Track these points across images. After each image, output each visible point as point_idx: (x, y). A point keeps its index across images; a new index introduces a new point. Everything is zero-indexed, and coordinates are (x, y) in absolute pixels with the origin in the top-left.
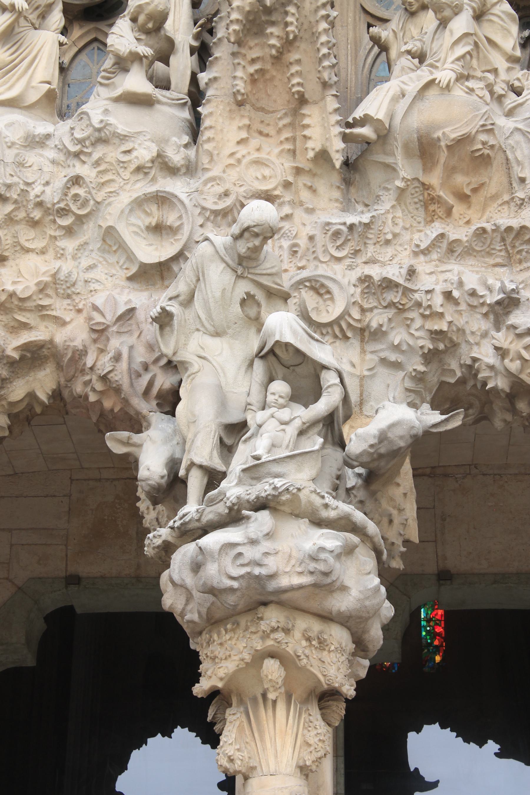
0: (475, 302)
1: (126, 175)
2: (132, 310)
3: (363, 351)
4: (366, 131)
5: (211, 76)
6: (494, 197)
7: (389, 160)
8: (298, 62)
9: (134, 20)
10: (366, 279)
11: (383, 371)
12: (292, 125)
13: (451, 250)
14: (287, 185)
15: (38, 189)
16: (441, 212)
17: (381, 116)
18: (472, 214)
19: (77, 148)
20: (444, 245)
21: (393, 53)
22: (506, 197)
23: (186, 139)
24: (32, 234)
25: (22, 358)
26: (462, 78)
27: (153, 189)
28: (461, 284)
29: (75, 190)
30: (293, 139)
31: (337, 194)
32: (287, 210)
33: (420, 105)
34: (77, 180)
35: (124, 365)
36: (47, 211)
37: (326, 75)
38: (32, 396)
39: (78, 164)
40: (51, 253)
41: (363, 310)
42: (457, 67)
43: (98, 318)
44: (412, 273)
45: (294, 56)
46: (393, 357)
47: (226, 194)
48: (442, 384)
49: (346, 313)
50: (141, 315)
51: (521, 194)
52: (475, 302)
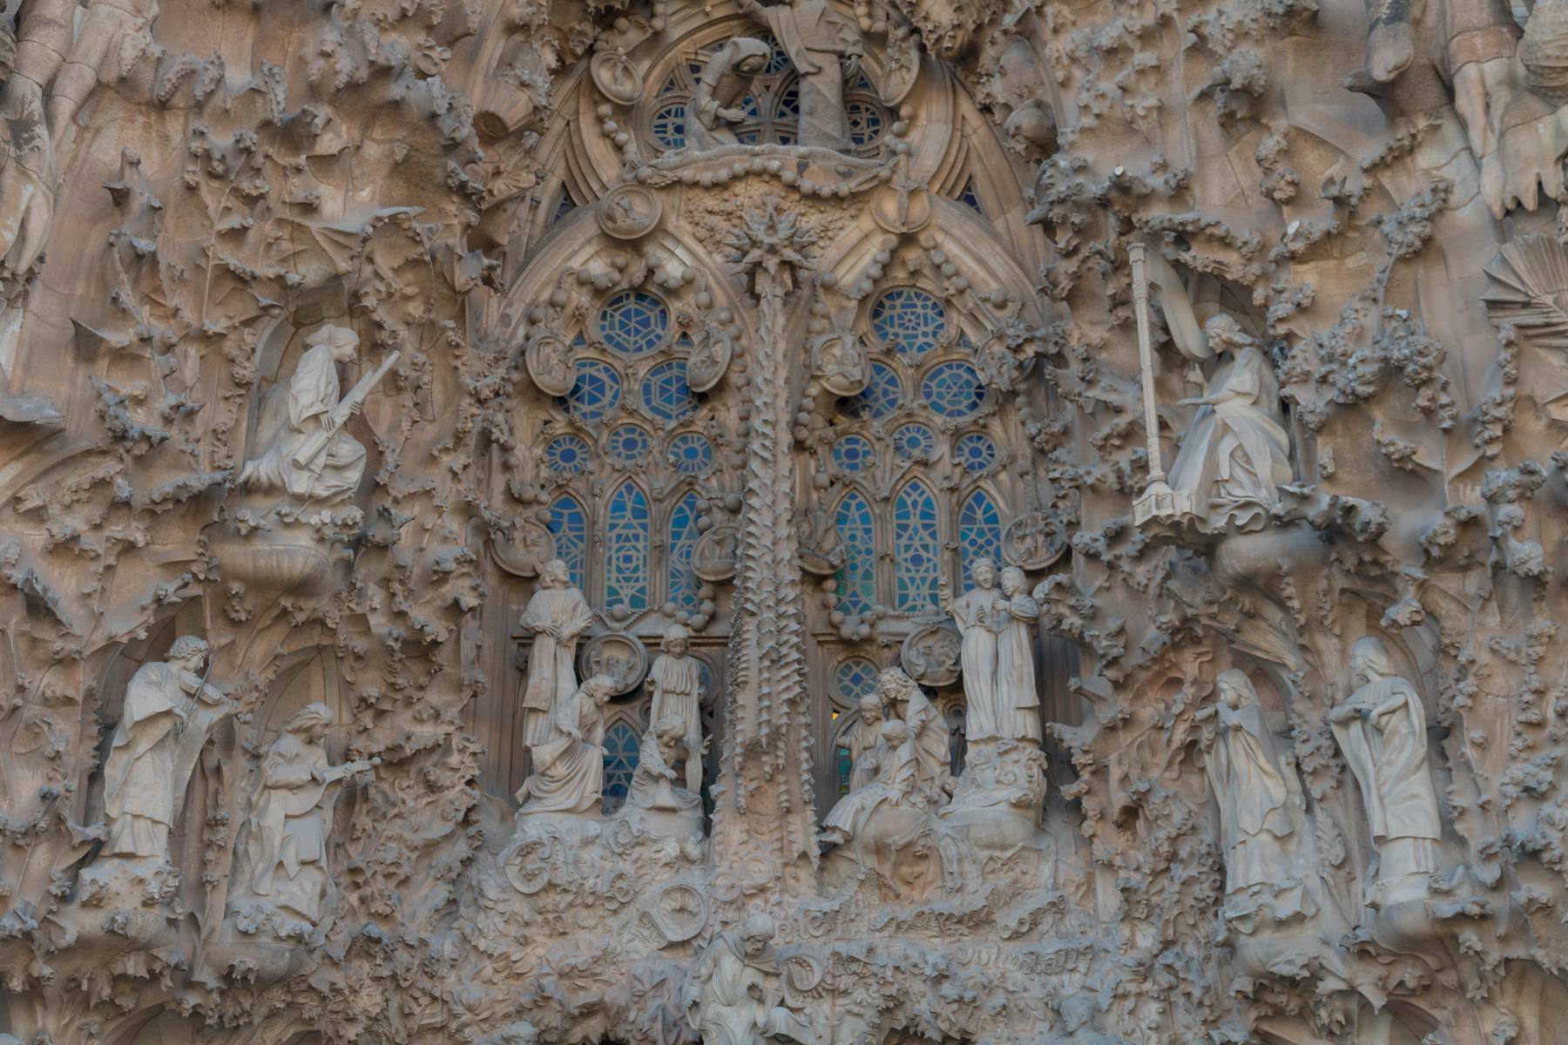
0: (916, 971)
1: (657, 868)
2: (663, 981)
3: (834, 1005)
4: (836, 838)
5: (722, 789)
6: (931, 882)
7: (853, 856)
8: (786, 782)
9: (660, 737)
10: (835, 954)
11: (848, 1018)
12: (780, 827)
13: (898, 927)
14: (778, 878)
15: (589, 883)
16: (891, 895)
17: (847, 828)
18: (916, 894)
19: (620, 850)
20: (894, 925)
21: (854, 754)
22: (939, 883)
23: (700, 835)
24: (585, 913)
25: (581, 1014)
26: (906, 794)
27: (678, 881)
28: (906, 958)
29: (620, 884)
30: (782, 838)
31: (813, 882)
32: (775, 898)
33: (876, 817)
34: (620, 876)
35: (658, 1026)
36: (598, 898)
37: (806, 797)
38: (586, 1037)
39: (621, 863)
40: (600, 929)
41: (834, 977)
42: (904, 787)
43: (640, 987)
44: (870, 951)
45: (781, 778)
46: (856, 1009)
47: (733, 887)
48: (893, 1030)
49: (823, 980)
50: (671, 984)
51: (949, 884)
52: (916, 971)
